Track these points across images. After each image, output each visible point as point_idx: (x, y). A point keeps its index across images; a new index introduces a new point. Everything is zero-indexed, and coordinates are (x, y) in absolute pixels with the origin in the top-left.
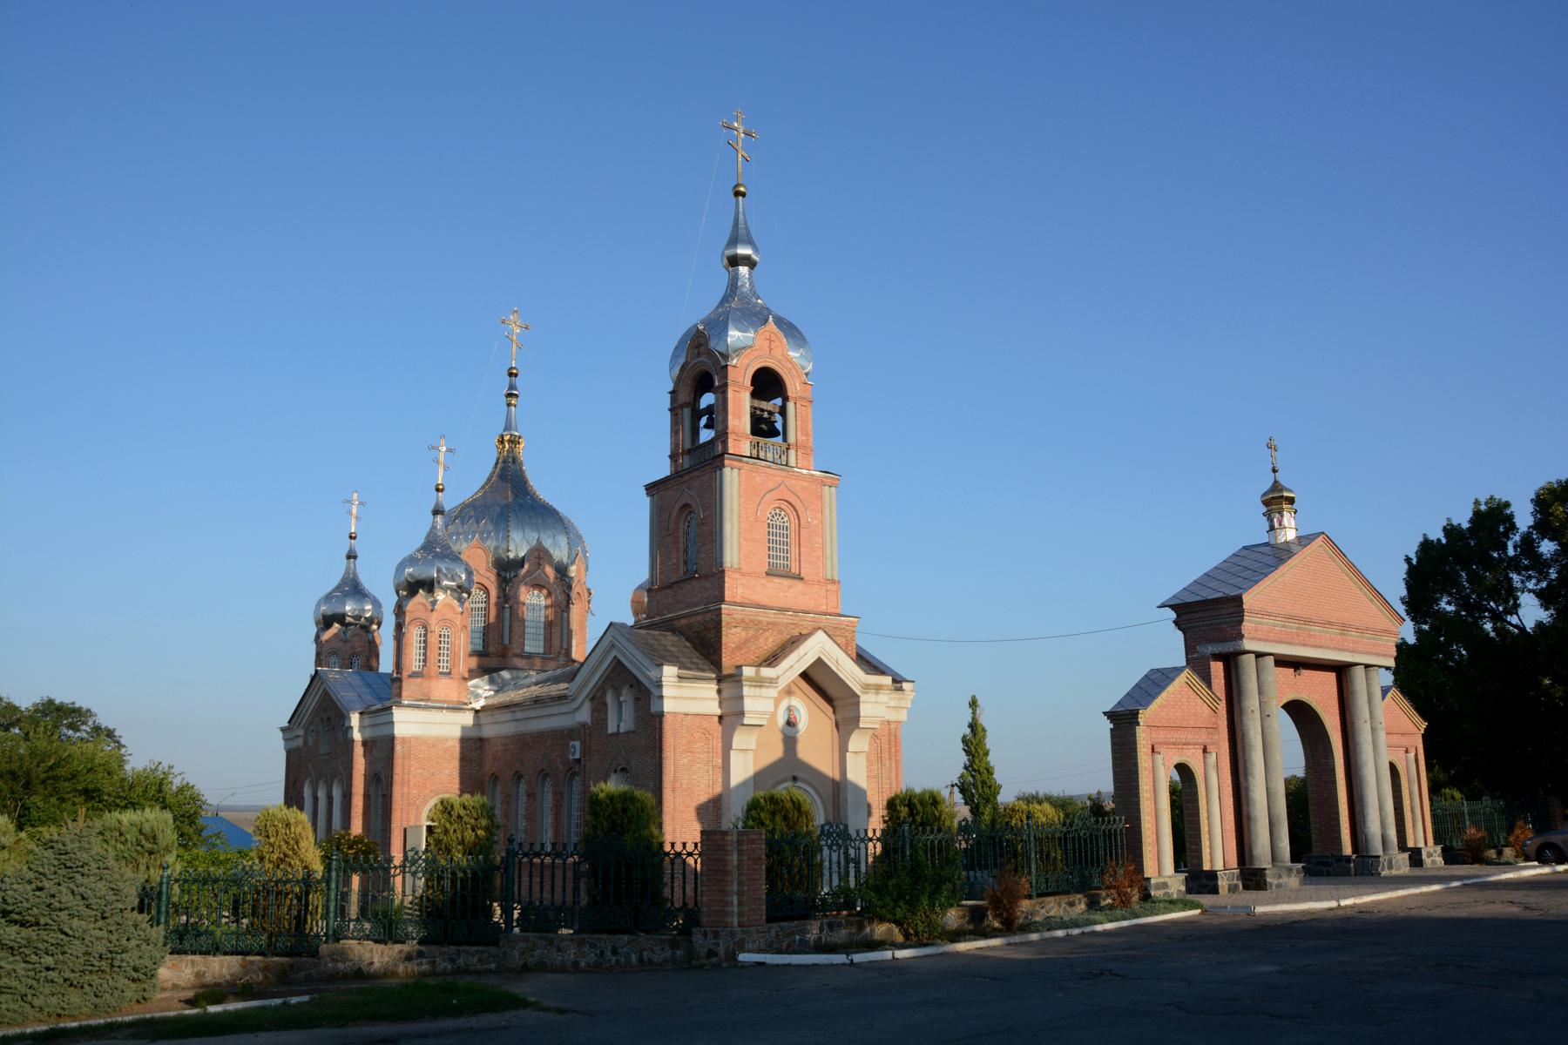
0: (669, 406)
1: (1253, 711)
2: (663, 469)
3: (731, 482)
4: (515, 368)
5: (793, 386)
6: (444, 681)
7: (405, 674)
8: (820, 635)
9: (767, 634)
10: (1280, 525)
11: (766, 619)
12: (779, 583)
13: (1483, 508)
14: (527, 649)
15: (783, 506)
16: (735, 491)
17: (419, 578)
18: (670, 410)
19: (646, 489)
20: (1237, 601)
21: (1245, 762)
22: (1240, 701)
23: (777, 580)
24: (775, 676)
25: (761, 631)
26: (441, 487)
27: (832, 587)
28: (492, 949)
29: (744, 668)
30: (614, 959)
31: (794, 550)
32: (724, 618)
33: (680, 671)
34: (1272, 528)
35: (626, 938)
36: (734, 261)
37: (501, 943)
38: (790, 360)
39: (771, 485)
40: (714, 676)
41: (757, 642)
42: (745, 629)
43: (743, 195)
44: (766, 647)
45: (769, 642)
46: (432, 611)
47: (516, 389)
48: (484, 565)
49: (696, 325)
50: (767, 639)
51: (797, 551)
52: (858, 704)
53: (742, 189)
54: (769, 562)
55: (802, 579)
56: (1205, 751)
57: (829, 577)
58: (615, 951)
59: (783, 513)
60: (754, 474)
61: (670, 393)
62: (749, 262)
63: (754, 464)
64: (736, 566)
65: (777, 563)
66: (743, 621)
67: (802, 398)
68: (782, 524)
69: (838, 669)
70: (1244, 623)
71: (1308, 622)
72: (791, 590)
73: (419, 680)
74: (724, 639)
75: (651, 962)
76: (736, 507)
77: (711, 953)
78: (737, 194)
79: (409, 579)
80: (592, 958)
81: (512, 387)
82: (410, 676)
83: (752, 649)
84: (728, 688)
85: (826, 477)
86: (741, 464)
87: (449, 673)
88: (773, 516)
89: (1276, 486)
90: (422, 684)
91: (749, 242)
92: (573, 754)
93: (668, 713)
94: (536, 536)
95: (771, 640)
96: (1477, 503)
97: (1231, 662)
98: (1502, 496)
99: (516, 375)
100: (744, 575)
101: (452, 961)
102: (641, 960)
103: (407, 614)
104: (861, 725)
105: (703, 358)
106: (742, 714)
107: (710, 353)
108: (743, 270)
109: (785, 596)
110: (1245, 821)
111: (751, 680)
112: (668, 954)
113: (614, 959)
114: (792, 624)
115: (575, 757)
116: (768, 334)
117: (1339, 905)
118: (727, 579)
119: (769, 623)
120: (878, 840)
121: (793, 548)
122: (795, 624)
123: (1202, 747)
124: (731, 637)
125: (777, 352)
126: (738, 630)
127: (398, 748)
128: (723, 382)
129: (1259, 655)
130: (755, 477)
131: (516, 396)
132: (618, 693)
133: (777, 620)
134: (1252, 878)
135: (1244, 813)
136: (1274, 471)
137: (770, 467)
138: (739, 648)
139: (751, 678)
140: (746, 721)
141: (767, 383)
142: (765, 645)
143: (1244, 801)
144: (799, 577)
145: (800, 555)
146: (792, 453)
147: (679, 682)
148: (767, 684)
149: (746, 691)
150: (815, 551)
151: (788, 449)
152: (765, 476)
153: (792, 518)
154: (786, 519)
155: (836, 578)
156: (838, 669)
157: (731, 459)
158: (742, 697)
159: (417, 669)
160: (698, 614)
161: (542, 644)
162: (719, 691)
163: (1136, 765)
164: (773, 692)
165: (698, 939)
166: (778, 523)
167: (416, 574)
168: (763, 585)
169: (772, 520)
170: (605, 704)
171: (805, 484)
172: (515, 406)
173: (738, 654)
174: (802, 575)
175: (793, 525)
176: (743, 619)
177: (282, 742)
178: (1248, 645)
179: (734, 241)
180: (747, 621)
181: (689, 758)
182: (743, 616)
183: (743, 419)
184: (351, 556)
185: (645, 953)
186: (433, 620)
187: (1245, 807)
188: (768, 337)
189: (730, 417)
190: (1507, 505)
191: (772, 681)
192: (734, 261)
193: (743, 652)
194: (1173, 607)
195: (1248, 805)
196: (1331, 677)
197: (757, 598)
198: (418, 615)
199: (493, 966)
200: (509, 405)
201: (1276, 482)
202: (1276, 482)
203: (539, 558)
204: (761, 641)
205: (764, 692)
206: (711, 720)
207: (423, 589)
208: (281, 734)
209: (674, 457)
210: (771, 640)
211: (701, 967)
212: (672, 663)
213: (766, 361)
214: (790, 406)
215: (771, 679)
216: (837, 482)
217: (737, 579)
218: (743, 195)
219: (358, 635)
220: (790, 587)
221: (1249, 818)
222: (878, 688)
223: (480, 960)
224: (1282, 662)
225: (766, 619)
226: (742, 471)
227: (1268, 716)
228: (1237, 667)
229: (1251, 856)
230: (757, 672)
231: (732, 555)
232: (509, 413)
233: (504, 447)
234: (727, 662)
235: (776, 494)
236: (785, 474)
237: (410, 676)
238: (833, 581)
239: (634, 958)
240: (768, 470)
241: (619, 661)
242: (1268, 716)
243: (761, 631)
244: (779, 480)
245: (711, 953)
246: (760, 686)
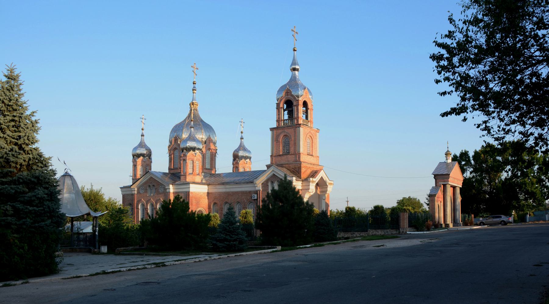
0: (276, 107)
2: (275, 125)
4: (195, 81)
5: (309, 106)
7: (187, 174)
13: (464, 152)
14: (207, 167)
15: (309, 137)
18: (276, 108)
19: (270, 129)
20: (449, 174)
21: (446, 204)
22: (446, 193)
23: (309, 156)
27: (318, 158)
28: (367, 233)
30: (387, 233)
32: (302, 165)
34: (447, 159)
35: (389, 230)
36: (294, 69)
37: (368, 231)
38: (309, 98)
39: (308, 132)
43: (296, 51)
45: (309, 172)
46: (195, 156)
47: (196, 88)
49: (285, 86)
52: (327, 188)
53: (296, 49)
55: (313, 156)
56: (441, 202)
58: (387, 232)
61: (276, 103)
62: (298, 70)
66: (305, 166)
71: (455, 179)
73: (192, 176)
74: (302, 171)
75: (393, 234)
77: (403, 232)
78: (294, 50)
79: (188, 147)
80: (383, 233)
81: (194, 87)
84: (305, 183)
87: (199, 174)
89: (448, 151)
91: (298, 65)
92: (254, 197)
96: (462, 151)
97: (445, 186)
98: (467, 150)
99: (195, 84)
101: (360, 234)
102: (391, 233)
103: (187, 157)
104: (327, 193)
105: (289, 96)
106: (309, 189)
107: (292, 96)
108: (296, 72)
110: (445, 215)
112: (395, 232)
113: (387, 233)
115: (255, 198)
118: (301, 156)
124: (303, 170)
125: (307, 96)
127: (191, 195)
128: (297, 104)
129: (449, 184)
131: (196, 90)
132: (272, 182)
134: (447, 226)
135: (445, 214)
136: (448, 148)
138: (304, 173)
140: (309, 191)
141: (305, 104)
143: (445, 212)
144: (312, 155)
145: (312, 150)
146: (309, 123)
149: (311, 184)
152: (307, 130)
158: (309, 185)
160: (293, 164)
161: (209, 165)
162: (302, 183)
163: (435, 204)
165: (401, 230)
170: (268, 185)
171: (313, 132)
174: (313, 155)
177: (121, 192)
178: (450, 183)
179: (294, 63)
184: (142, 135)
185: (392, 232)
186: (195, 159)
187: (445, 213)
189: (299, 114)
190: (468, 152)
192: (294, 69)
194: (434, 175)
195: (446, 212)
198: (191, 157)
199: (367, 235)
200: (193, 93)
201: (448, 150)
202: (448, 150)
207: (192, 150)
208: (120, 189)
209: (278, 121)
211: (402, 234)
212: (295, 177)
214: (309, 111)
218: (296, 51)
219: (148, 160)
220: (311, 158)
221: (446, 215)
222: (331, 184)
223: (365, 234)
228: (446, 187)
229: (446, 222)
231: (302, 150)
234: (304, 176)
236: (310, 129)
238: (318, 157)
239: (390, 233)
240: (308, 128)
241: (274, 174)
244: (309, 131)
245: (403, 232)
246: (313, 183)
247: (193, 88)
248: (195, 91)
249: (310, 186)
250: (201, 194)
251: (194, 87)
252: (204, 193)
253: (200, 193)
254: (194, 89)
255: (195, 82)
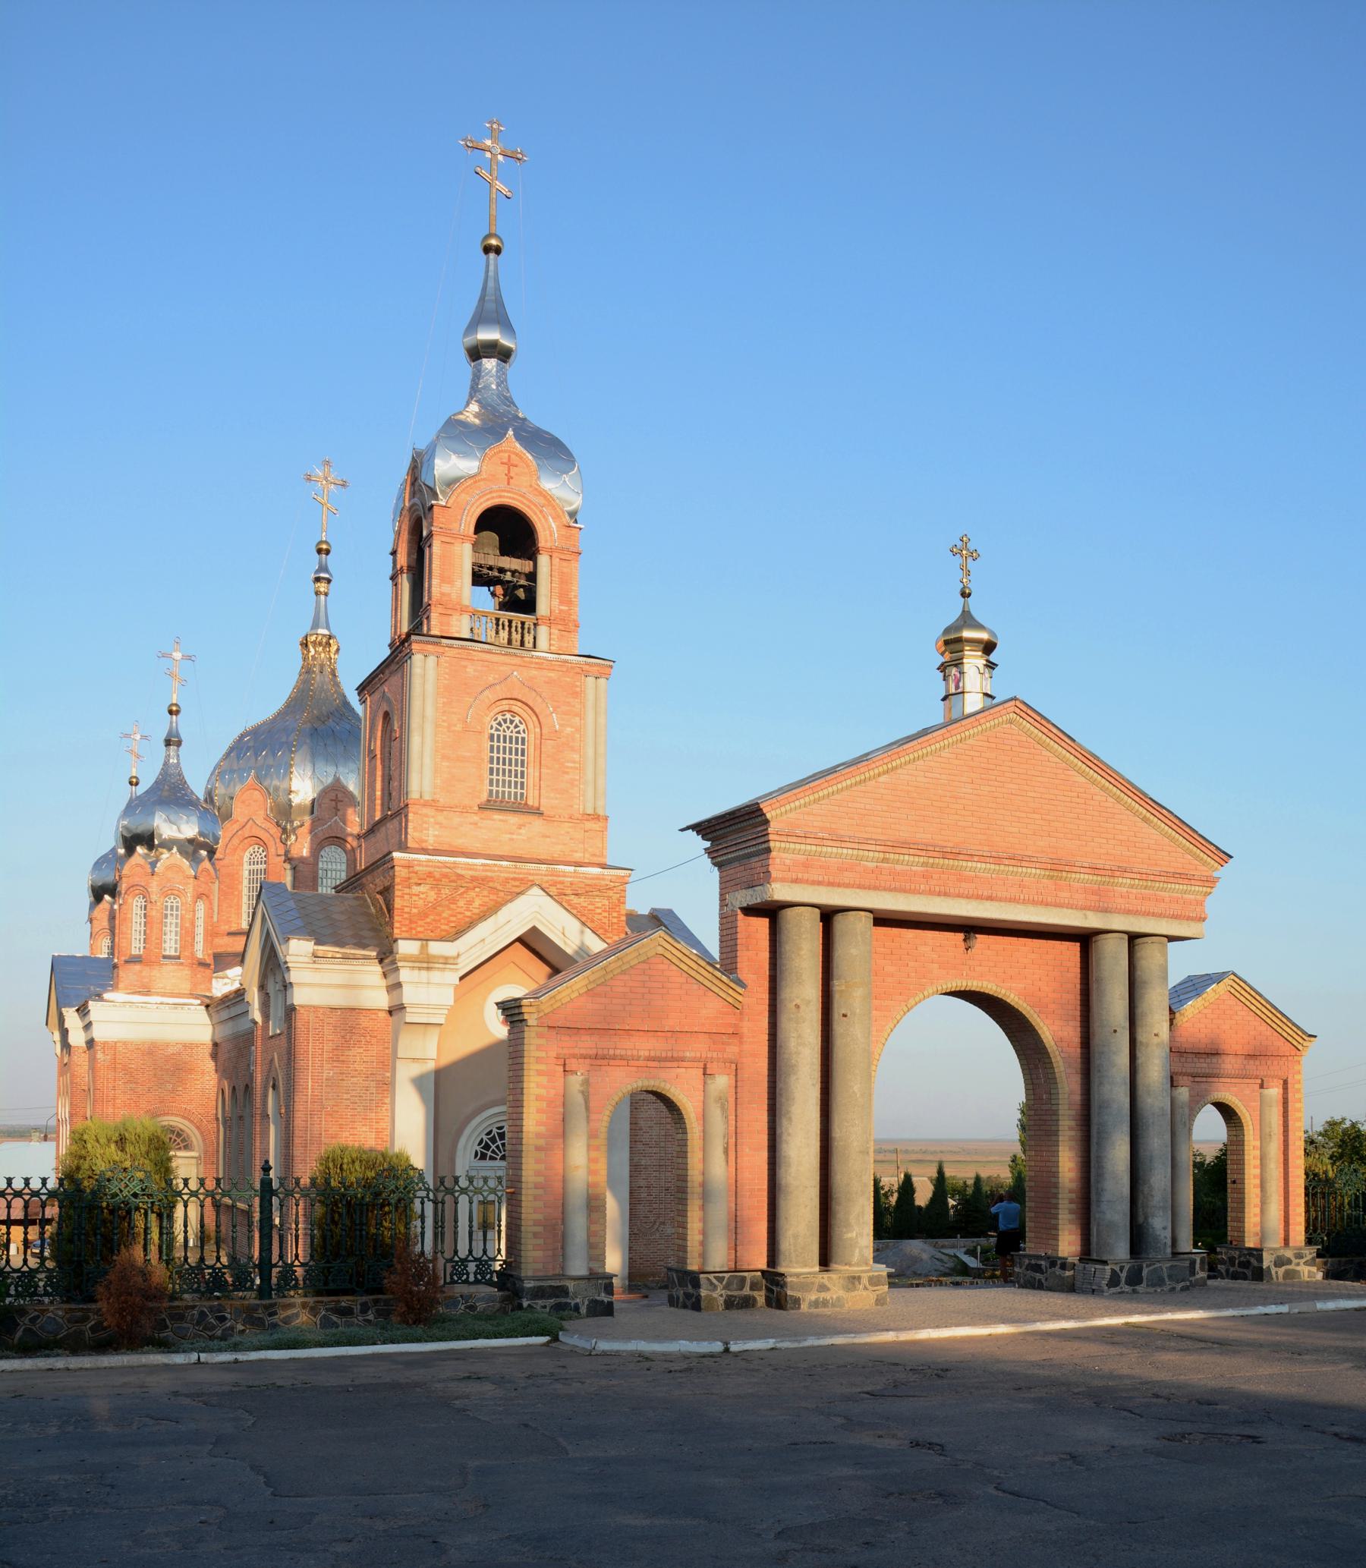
1: (797, 1006)
3: (424, 676)
4: (326, 542)
6: (169, 968)
8: (536, 890)
9: (472, 894)
10: (957, 687)
11: (471, 873)
12: (501, 820)
15: (515, 709)
16: (430, 688)
17: (135, 831)
24: (455, 954)
25: (462, 890)
26: (174, 708)
29: (399, 941)
31: (532, 772)
33: (316, 947)
40: (374, 954)
41: (452, 906)
42: (436, 886)
44: (468, 914)
48: (262, 812)
50: (470, 902)
51: (537, 774)
54: (491, 791)
57: (590, 811)
59: (517, 719)
60: (464, 663)
63: (463, 648)
64: (427, 797)
65: (497, 792)
66: (430, 875)
67: (562, 550)
68: (514, 735)
69: (565, 943)
70: (773, 854)
72: (523, 831)
76: (430, 711)
81: (323, 568)
82: (126, 962)
83: (445, 915)
85: (587, 664)
86: (440, 649)
88: (500, 724)
90: (141, 972)
93: (302, 1006)
94: (331, 770)
95: (477, 903)
99: (328, 552)
100: (440, 809)
109: (512, 839)
111: (408, 959)
114: (514, 879)
116: (506, 455)
117: (727, 1350)
119: (474, 879)
120: (180, 1194)
121: (531, 770)
122: (522, 879)
123: (701, 1065)
126: (422, 888)
130: (466, 667)
133: (489, 874)
137: (489, 652)
139: (412, 956)
142: (468, 910)
144: (537, 812)
147: (314, 962)
148: (441, 966)
150: (567, 773)
151: (535, 625)
153: (531, 726)
154: (522, 727)
155: (600, 812)
156: (565, 943)
157: (421, 642)
159: (137, 953)
164: (454, 978)
166: (508, 733)
167: (133, 827)
168: (476, 824)
169: (497, 730)
172: (326, 594)
173: (421, 923)
175: (532, 736)
176: (430, 873)
180: (437, 875)
181: (336, 1070)
182: (432, 869)
183: (458, 583)
188: (505, 461)
191: (447, 961)
193: (428, 920)
196: (1073, 950)
197: (460, 842)
198: (136, 880)
200: (317, 593)
203: (336, 800)
204: (461, 903)
205: (436, 976)
206: (373, 1016)
210: (477, 903)
213: (500, 497)
215: (446, 958)
216: (607, 670)
217: (426, 816)
220: (520, 827)
224: (884, 920)
225: (471, 873)
226: (442, 659)
227: (845, 1016)
230: (424, 948)
232: (318, 603)
233: (309, 651)
235: (501, 691)
237: (126, 962)
238: (596, 817)
242: (845, 1016)
243: (462, 890)
246: (428, 969)
247: (317, 572)
248: (322, 587)
249: (406, 988)
250: (171, 1051)
251: (323, 568)
252: (189, 1047)
253: (168, 1045)
254: (322, 575)
255: (324, 546)
